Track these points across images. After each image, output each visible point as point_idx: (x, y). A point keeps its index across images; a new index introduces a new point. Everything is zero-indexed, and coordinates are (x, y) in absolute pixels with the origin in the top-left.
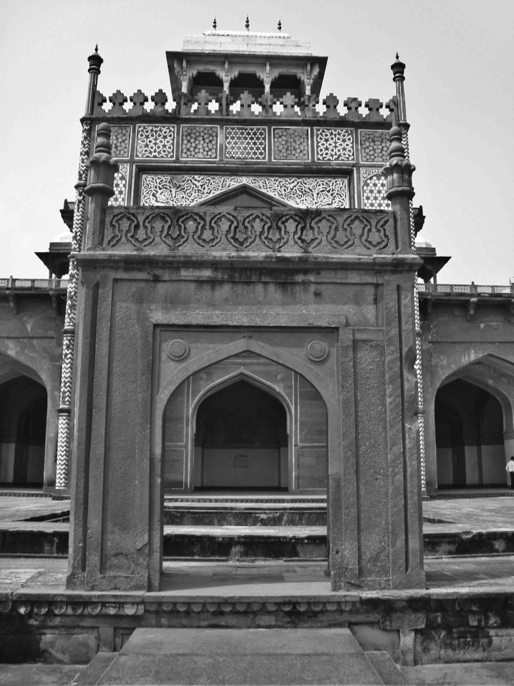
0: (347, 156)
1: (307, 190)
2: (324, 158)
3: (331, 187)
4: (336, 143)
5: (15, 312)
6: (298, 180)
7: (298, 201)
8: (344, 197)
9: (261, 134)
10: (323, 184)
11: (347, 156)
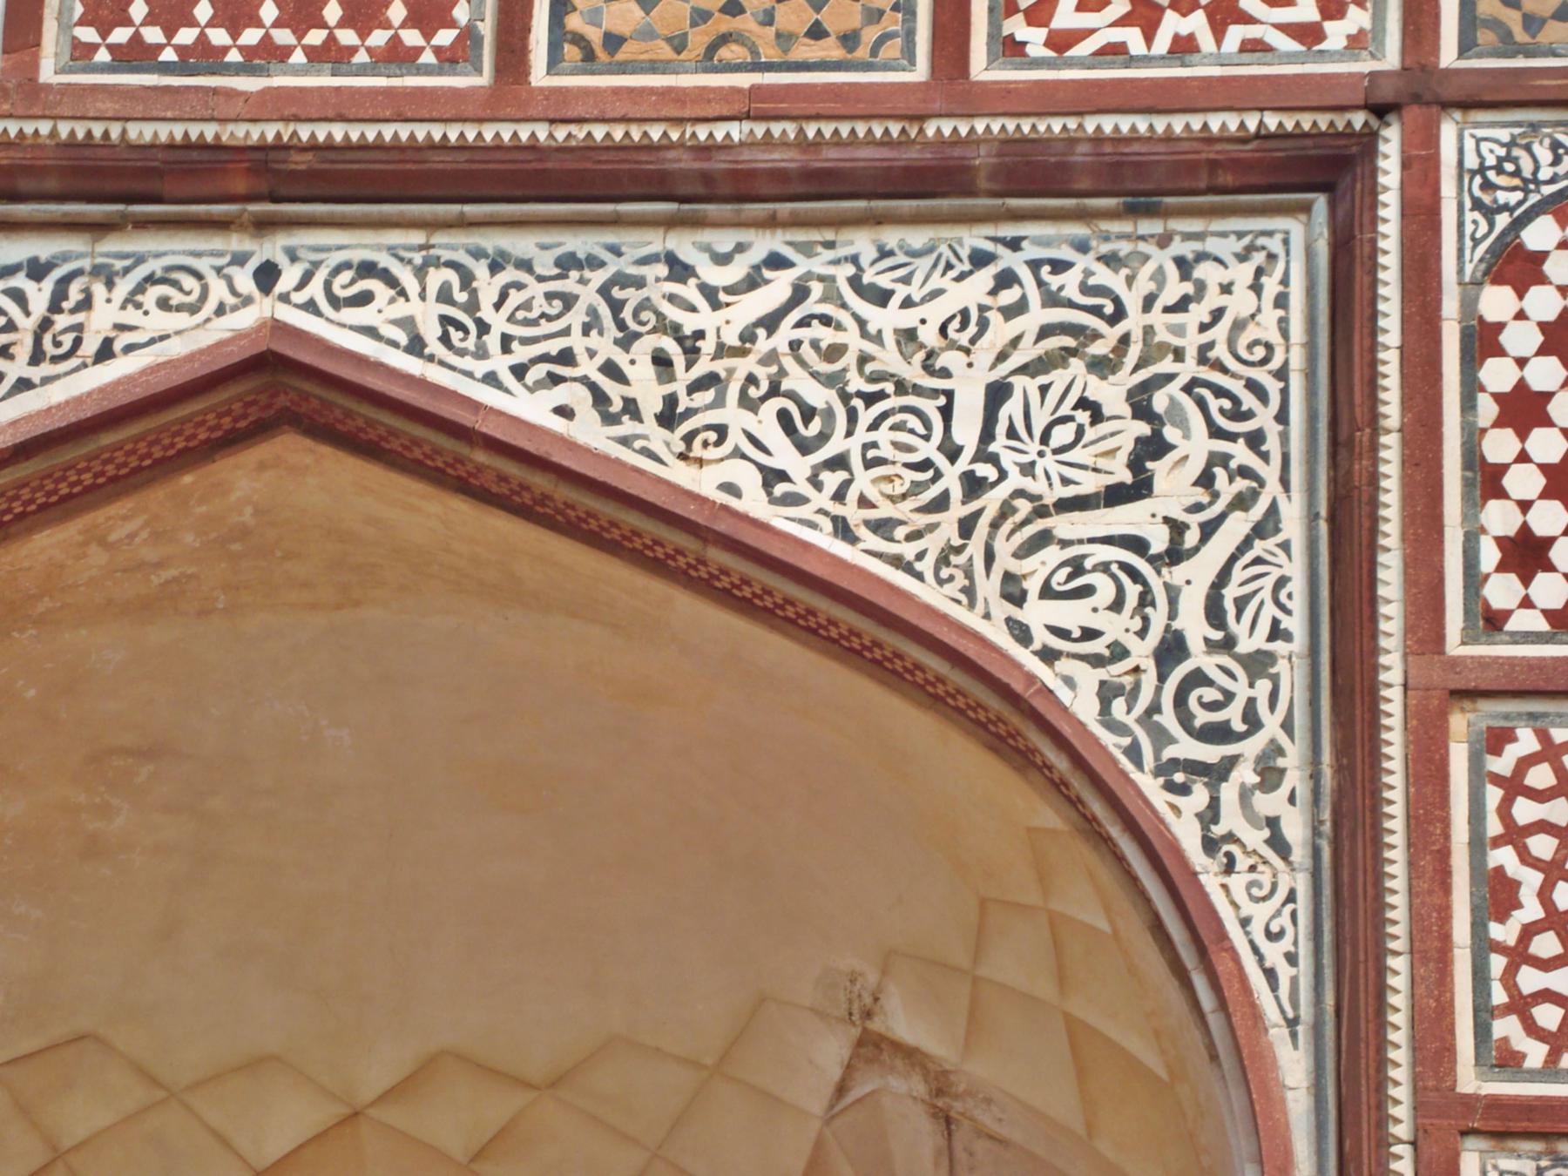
1: (889, 358)
2: (1061, 42)
3: (1133, 323)
6: (803, 265)
7: (798, 466)
8: (1264, 418)
10: (1052, 299)
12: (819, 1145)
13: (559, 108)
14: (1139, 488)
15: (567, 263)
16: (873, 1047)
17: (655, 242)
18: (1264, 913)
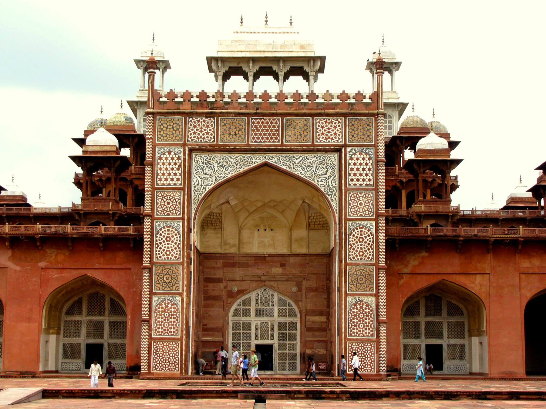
0: (337, 139)
1: (309, 164)
2: (321, 141)
4: (329, 129)
5: (102, 249)
7: (303, 172)
9: (276, 123)
11: (337, 139)
12: (299, 208)
13: (286, 146)
14: (326, 174)
15: (286, 156)
16: (304, 202)
17: (292, 155)
18: (335, 204)
